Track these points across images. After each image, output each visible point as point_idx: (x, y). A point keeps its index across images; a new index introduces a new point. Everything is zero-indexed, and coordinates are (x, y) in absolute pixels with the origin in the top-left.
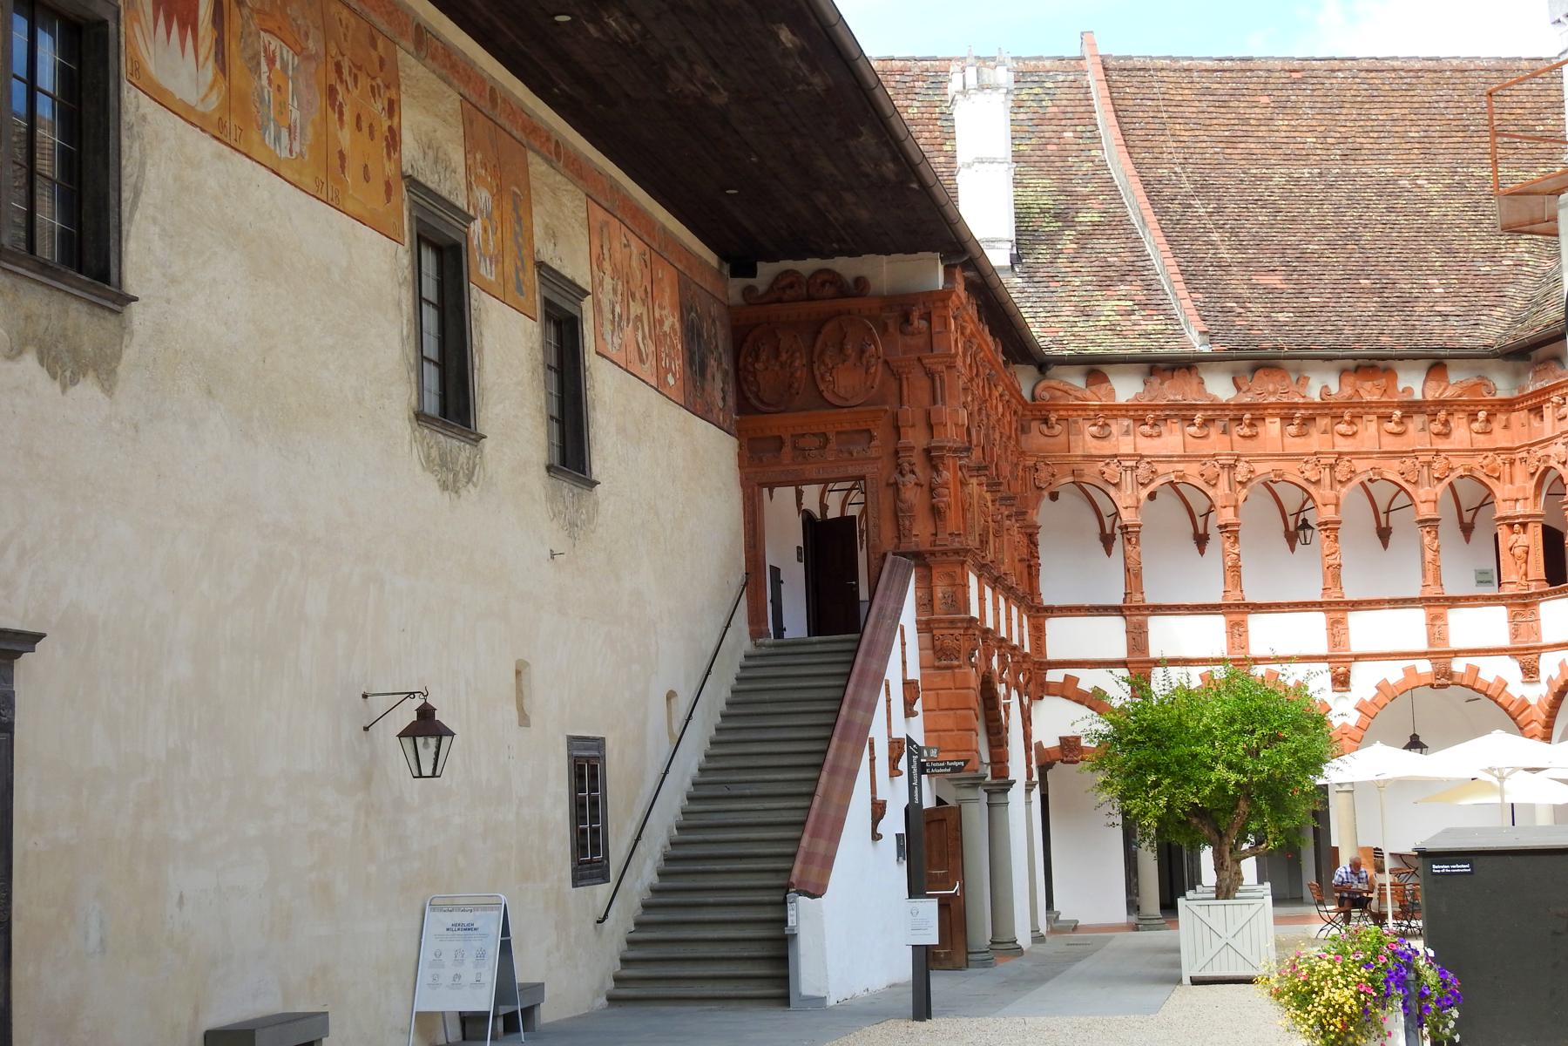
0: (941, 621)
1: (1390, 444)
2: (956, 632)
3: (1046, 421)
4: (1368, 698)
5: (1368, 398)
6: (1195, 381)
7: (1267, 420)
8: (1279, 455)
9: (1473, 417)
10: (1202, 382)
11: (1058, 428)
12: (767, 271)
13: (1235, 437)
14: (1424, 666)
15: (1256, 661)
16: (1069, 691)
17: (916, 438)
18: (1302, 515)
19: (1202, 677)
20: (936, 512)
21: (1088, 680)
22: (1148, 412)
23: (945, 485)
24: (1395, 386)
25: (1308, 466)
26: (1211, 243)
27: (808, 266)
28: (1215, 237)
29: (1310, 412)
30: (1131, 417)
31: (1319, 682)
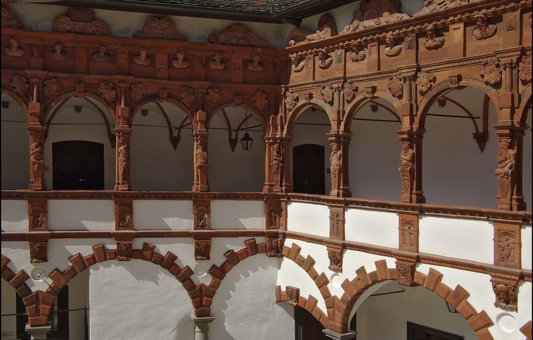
7: (452, 27)
8: (459, 61)
13: (422, 49)
15: (419, 259)
19: (377, 263)
22: (353, 41)
25: (488, 68)
29: (493, 9)
30: (342, 47)
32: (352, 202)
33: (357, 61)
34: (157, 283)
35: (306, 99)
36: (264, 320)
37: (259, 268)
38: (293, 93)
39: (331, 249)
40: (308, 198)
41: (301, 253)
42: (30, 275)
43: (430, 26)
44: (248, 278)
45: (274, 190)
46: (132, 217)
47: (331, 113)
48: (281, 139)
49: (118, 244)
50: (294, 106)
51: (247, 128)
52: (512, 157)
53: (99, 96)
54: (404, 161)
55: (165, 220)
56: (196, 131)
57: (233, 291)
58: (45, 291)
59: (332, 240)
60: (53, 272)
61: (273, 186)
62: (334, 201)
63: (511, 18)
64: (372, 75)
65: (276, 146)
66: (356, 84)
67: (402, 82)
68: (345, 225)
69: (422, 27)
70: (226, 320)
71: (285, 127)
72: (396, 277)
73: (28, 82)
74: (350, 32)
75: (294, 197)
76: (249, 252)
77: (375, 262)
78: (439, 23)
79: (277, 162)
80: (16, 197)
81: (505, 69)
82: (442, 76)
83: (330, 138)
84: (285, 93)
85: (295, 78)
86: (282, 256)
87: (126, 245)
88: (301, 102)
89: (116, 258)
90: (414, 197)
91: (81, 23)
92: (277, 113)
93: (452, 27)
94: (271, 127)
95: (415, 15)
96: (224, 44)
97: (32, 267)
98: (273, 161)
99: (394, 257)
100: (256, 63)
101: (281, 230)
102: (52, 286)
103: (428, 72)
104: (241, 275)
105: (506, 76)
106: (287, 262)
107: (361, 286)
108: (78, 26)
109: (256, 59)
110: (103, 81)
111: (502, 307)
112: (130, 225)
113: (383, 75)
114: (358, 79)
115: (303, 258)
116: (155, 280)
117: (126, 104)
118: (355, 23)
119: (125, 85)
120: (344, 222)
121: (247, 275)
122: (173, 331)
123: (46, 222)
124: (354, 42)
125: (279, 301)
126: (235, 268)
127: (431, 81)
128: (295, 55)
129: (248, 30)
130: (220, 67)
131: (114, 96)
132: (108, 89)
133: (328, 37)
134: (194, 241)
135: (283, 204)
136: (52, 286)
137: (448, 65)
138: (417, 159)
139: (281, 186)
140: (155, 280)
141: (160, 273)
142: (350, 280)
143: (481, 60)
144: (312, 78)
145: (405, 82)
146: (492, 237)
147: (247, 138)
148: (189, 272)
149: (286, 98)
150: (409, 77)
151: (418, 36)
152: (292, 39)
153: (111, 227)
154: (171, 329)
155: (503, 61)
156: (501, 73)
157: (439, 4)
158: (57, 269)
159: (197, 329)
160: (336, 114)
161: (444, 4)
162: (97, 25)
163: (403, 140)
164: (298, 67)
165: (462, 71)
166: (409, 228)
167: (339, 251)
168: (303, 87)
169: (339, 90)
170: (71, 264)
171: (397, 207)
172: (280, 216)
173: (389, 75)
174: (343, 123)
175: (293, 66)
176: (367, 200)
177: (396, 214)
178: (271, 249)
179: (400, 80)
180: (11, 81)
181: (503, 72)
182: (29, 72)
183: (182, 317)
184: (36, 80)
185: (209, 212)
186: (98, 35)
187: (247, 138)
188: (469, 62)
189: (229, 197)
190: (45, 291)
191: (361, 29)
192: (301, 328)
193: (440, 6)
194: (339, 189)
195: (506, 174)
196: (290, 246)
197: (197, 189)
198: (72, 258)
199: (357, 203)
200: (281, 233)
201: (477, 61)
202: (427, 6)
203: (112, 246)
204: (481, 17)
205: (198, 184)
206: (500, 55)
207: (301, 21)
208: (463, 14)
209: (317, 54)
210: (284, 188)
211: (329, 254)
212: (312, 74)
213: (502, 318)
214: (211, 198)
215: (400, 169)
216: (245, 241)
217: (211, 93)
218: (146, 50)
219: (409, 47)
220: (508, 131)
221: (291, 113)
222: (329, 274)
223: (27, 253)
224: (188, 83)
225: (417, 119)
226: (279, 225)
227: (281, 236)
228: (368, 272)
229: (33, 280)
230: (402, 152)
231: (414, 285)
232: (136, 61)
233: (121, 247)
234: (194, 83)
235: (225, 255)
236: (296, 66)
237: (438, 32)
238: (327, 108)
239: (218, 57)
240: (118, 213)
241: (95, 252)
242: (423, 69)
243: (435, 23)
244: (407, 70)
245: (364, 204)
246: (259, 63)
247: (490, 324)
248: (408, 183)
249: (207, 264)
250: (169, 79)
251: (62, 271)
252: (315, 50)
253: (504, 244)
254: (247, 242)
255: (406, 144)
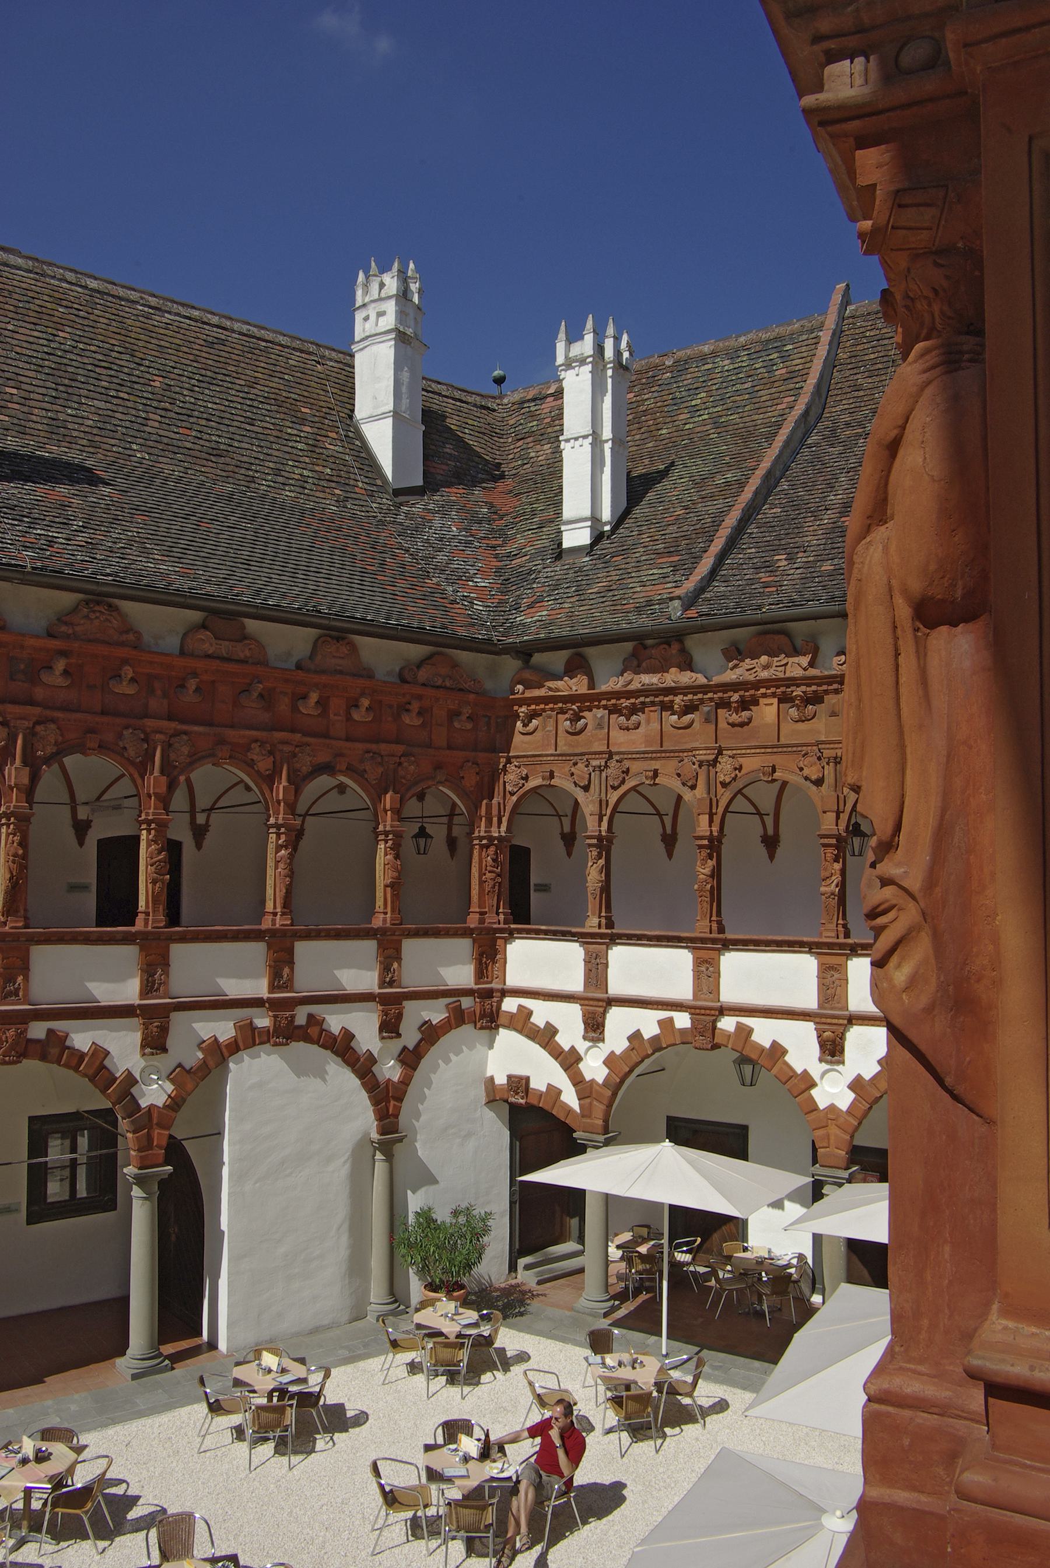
4: (867, 1076)
7: (762, 701)
8: (773, 747)
13: (722, 724)
15: (723, 1011)
32: (620, 936)
33: (628, 729)
34: (324, 1080)
35: (543, 779)
36: (469, 1135)
37: (464, 1048)
38: (519, 767)
39: (587, 1008)
40: (546, 932)
41: (533, 1019)
42: (138, 1078)
43: (736, 697)
44: (450, 1064)
45: (487, 921)
46: (292, 970)
47: (588, 805)
48: (500, 839)
49: (275, 1017)
50: (521, 788)
51: (422, 817)
52: (838, 872)
53: (250, 764)
54: (702, 876)
55: (338, 973)
56: (385, 826)
57: (429, 1089)
58: (161, 1105)
59: (590, 995)
60: (174, 1071)
61: (486, 913)
62: (592, 935)
63: (834, 701)
64: (652, 752)
65: (492, 849)
66: (627, 764)
67: (696, 766)
68: (609, 970)
69: (725, 695)
70: (418, 1137)
71: (505, 820)
72: (690, 1039)
73: (146, 740)
74: (618, 687)
75: (520, 931)
76: (453, 1022)
77: (658, 1021)
78: (747, 694)
79: (493, 875)
80: (122, 940)
81: (828, 764)
82: (751, 763)
83: (589, 841)
84: (505, 766)
85: (520, 743)
86: (497, 1027)
87: (287, 1018)
88: (533, 783)
89: (269, 1041)
90: (715, 926)
91: (227, 643)
92: (491, 798)
93: (762, 701)
94: (484, 819)
95: (717, 680)
96: (424, 685)
97: (142, 1063)
98: (485, 874)
99: (687, 1011)
100: (464, 717)
101: (495, 985)
102: (172, 1095)
103: (733, 757)
104: (440, 1061)
105: (829, 770)
106: (505, 1036)
107: (636, 1058)
108: (224, 648)
109: (467, 711)
110: (256, 741)
111: (827, 1062)
112: (288, 986)
113: (668, 755)
114: (630, 756)
115: (538, 1027)
116: (321, 1074)
117: (289, 780)
118: (628, 676)
119: (287, 748)
120: (606, 965)
121: (448, 1061)
122: (345, 1162)
123: (166, 983)
124: (625, 703)
125: (491, 1102)
126: (432, 1048)
127: (736, 769)
128: (524, 709)
129: (455, 665)
130: (417, 722)
131: (271, 766)
132: (263, 755)
133: (583, 690)
134: (380, 1008)
135: (500, 942)
136: (172, 1095)
137: (758, 751)
138: (716, 873)
139: (498, 914)
140: (321, 1074)
141: (329, 1063)
142: (618, 1052)
143: (799, 749)
144: (554, 748)
145: (700, 766)
146: (816, 974)
147: (422, 833)
148: (371, 1060)
149: (505, 775)
150: (708, 761)
151: (718, 706)
152: (519, 683)
153: (259, 987)
154: (343, 1159)
155: (827, 753)
156: (823, 768)
157: (747, 670)
158: (180, 1065)
159: (379, 1156)
160: (597, 805)
161: (754, 670)
162: (251, 646)
163: (700, 847)
164: (528, 728)
165: (777, 760)
166: (707, 969)
167: (601, 1010)
168: (537, 759)
169: (600, 769)
170: (200, 1055)
171: (692, 940)
172: (494, 962)
173: (677, 754)
174: (605, 819)
175: (519, 724)
176: (646, 933)
177: (686, 951)
178: (483, 1016)
179: (694, 764)
180: (120, 736)
181: (826, 767)
182: (150, 723)
183: (359, 1137)
184: (159, 736)
185: (399, 959)
186: (253, 664)
187: (422, 833)
188: (785, 749)
189: (426, 933)
190: (161, 1105)
191: (635, 686)
192: (518, 1143)
193: (750, 672)
194: (600, 917)
195: (833, 894)
196: (514, 1010)
197: (385, 920)
198: (204, 1045)
199: (629, 937)
200: (498, 990)
201: (795, 749)
202: (732, 669)
203: (263, 1021)
204: (800, 696)
205: (386, 913)
206: (823, 746)
207: (531, 656)
208: (778, 687)
209: (562, 712)
210: (502, 917)
211: (584, 1016)
212: (553, 742)
213: (827, 1076)
214: (403, 935)
215: (696, 887)
216: (447, 1005)
217: (405, 764)
218: (318, 691)
219: (706, 719)
220: (834, 841)
221: (514, 798)
223: (136, 1037)
224: (373, 747)
225: (717, 819)
226: (492, 977)
227: (499, 994)
228: (646, 1036)
229: (143, 1086)
230: (698, 863)
231: (716, 1047)
232: (301, 709)
233: (280, 1022)
234: (384, 748)
235: (420, 1028)
236: (525, 725)
237: (745, 705)
238: (580, 795)
239: (415, 706)
240: (273, 964)
241: (239, 1032)
242: (724, 752)
243: (742, 693)
244: (705, 752)
245: (639, 937)
246: (468, 718)
247: (813, 1085)
248: (706, 906)
249: (396, 1046)
250: (348, 739)
251: (188, 1067)
252: (560, 705)
253: (827, 981)
254: (450, 1006)
255: (705, 852)
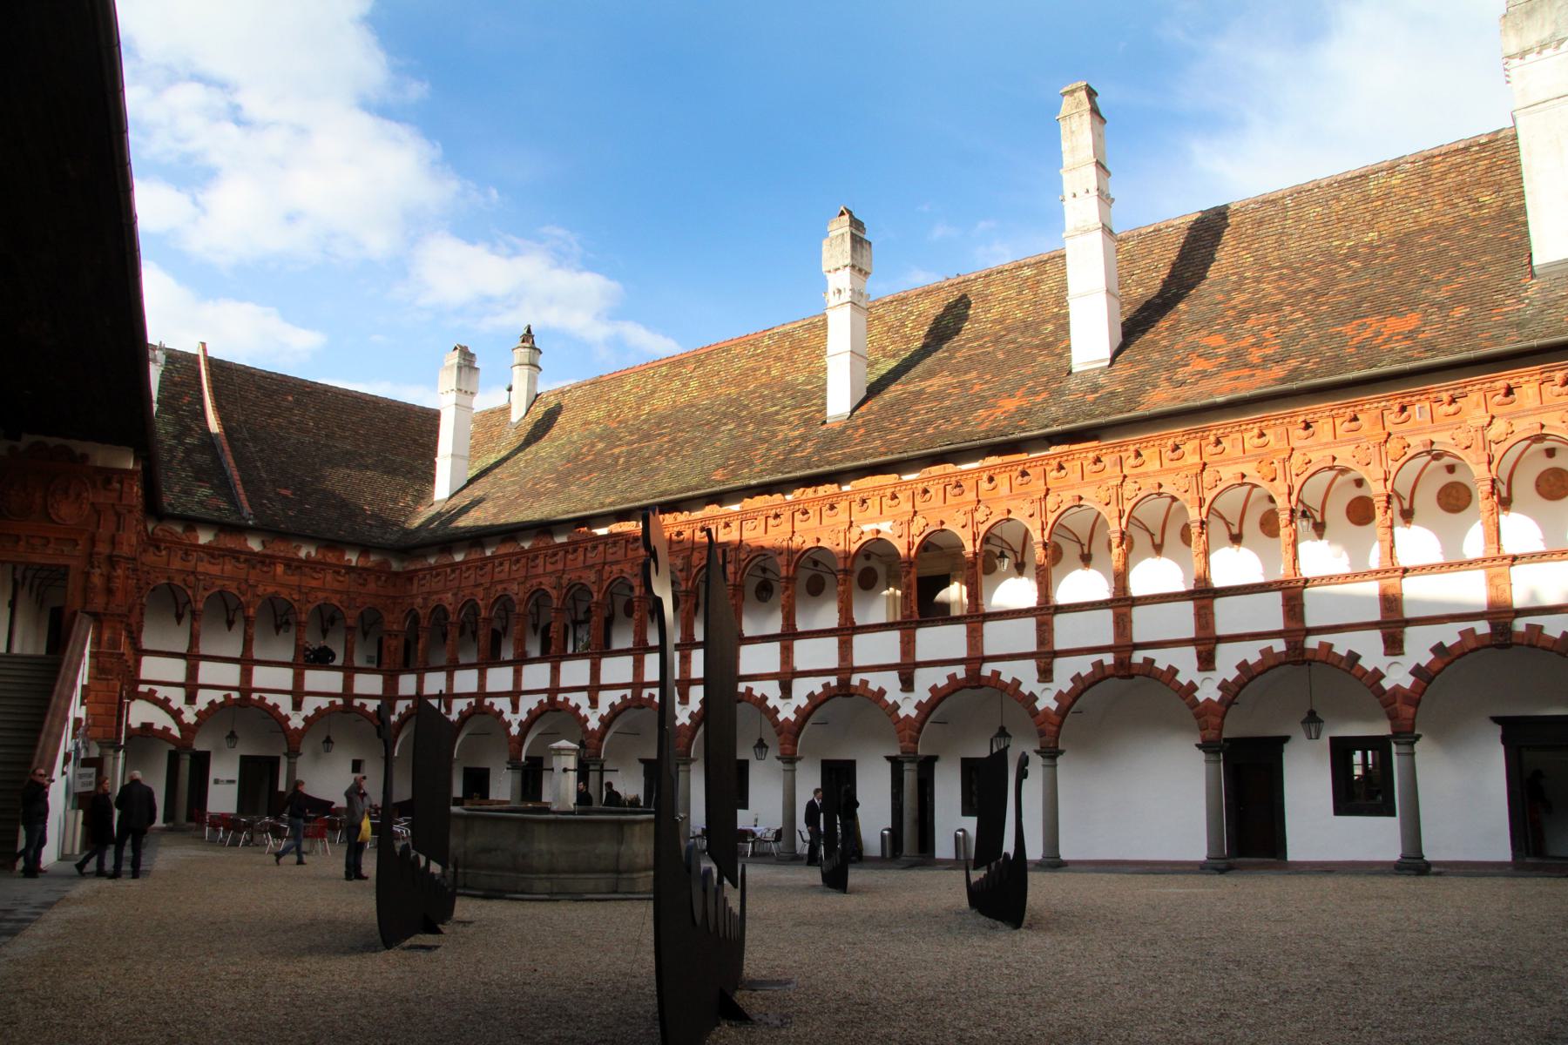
0: (102, 653)
1: (336, 585)
2: (114, 660)
3: (158, 548)
5: (328, 560)
6: (242, 539)
7: (278, 565)
9: (379, 578)
10: (246, 540)
11: (164, 553)
12: (27, 440)
14: (339, 701)
16: (150, 697)
17: (103, 548)
18: (285, 617)
20: (110, 591)
21: (162, 692)
23: (118, 577)
24: (343, 557)
26: (256, 467)
27: (53, 441)
28: (259, 464)
31: (285, 704)
43: (267, 561)
222: (184, 707)
